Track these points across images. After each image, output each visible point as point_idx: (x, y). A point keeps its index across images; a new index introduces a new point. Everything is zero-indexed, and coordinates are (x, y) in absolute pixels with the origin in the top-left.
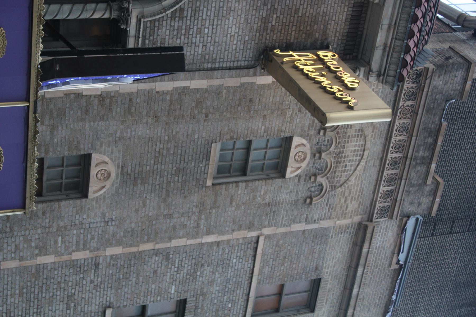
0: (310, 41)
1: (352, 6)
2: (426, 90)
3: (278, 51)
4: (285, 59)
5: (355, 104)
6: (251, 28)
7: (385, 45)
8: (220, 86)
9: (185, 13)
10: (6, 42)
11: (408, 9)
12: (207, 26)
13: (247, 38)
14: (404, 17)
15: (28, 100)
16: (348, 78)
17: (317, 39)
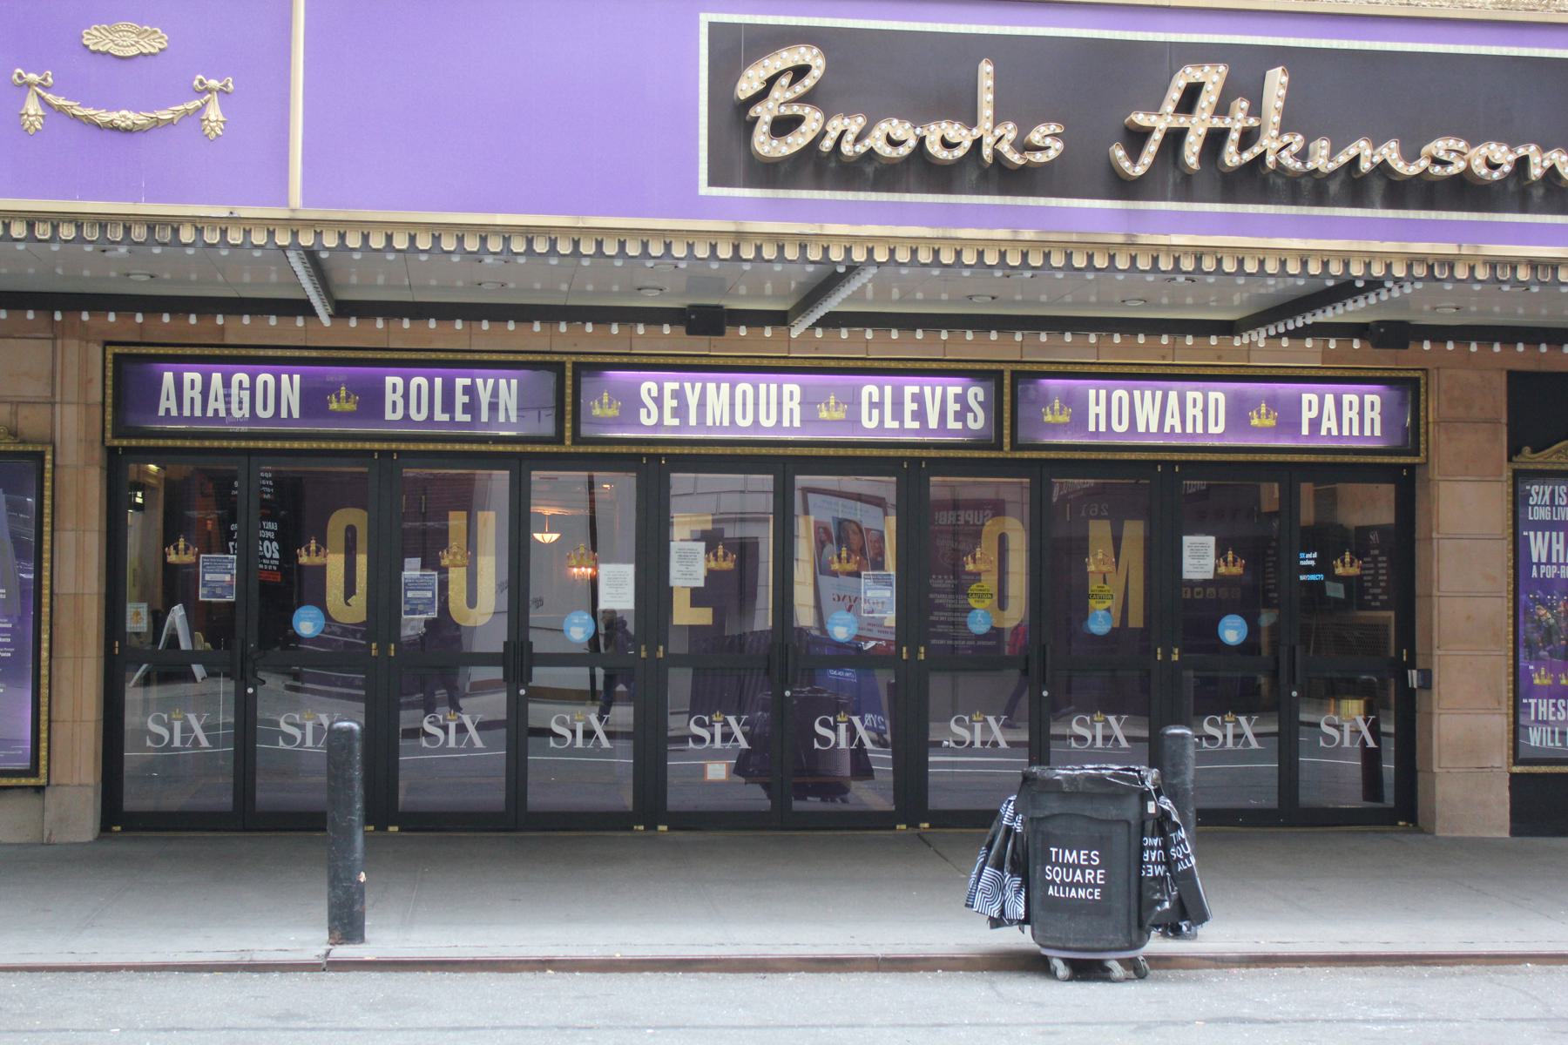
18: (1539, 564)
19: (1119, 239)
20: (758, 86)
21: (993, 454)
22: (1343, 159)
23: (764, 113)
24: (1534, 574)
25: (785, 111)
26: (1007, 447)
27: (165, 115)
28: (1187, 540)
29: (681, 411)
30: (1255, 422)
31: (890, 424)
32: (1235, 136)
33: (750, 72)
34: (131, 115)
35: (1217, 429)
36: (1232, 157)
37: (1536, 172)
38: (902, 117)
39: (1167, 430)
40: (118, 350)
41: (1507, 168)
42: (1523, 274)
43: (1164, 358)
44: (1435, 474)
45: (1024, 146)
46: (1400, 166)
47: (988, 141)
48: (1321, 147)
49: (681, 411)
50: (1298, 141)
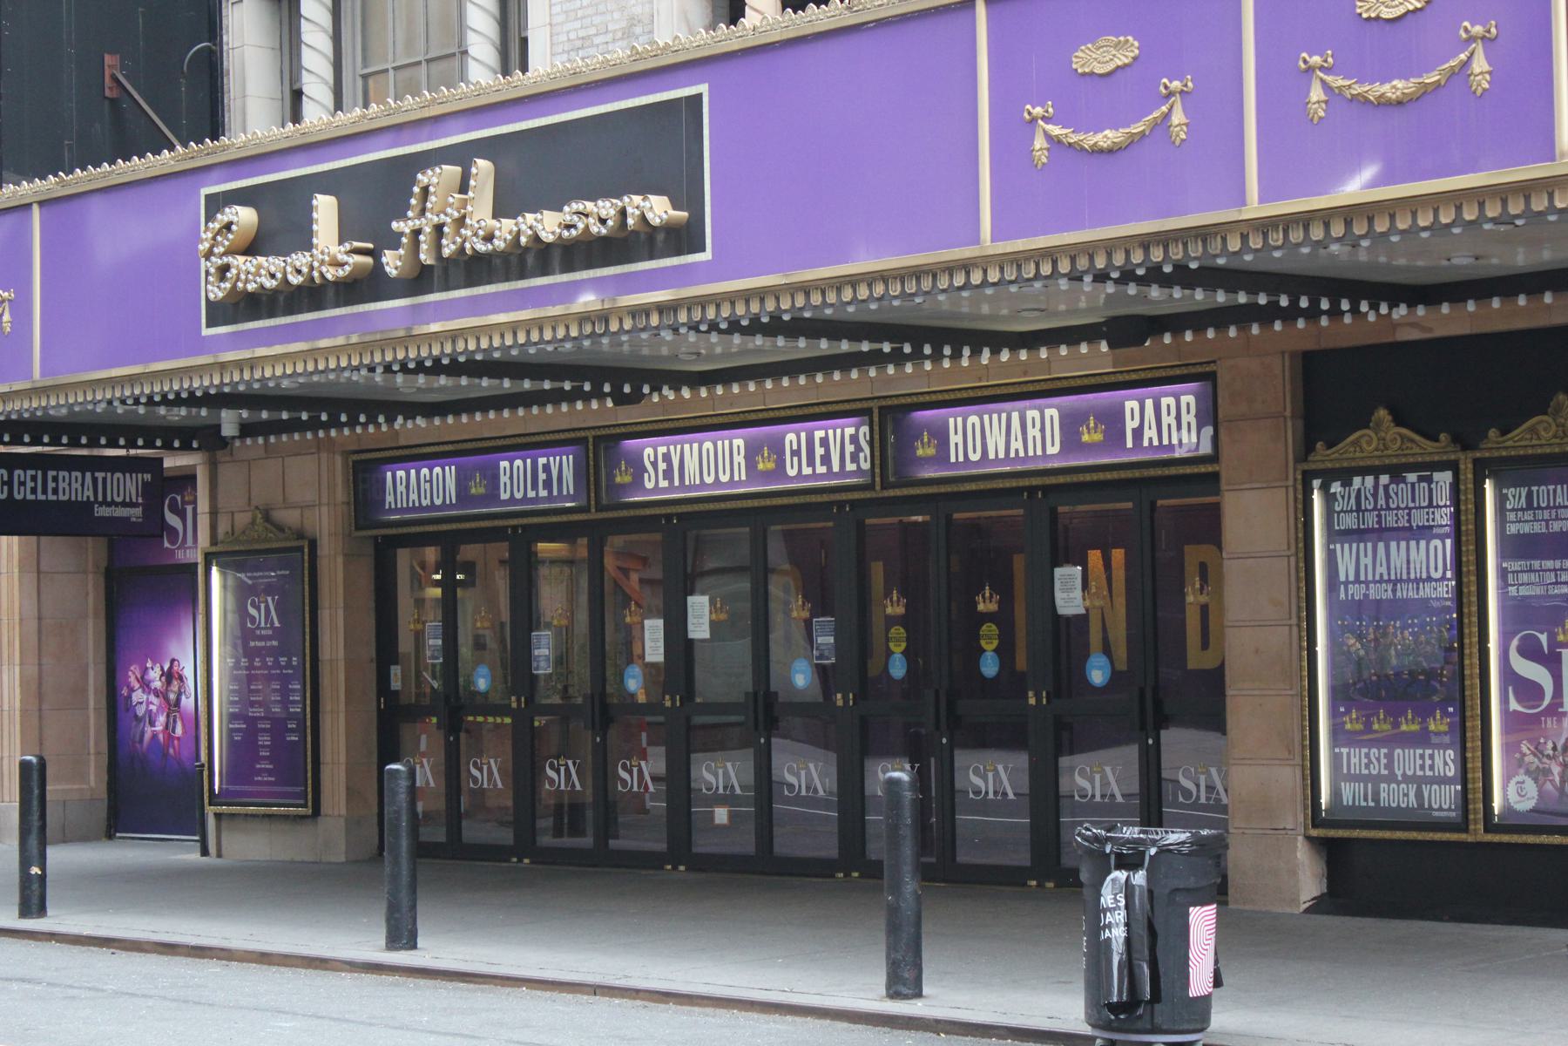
18: (1347, 583)
19: (401, 333)
21: (868, 495)
24: (1342, 596)
26: (878, 487)
28: (1058, 572)
29: (668, 474)
30: (1086, 438)
31: (807, 471)
35: (1053, 450)
39: (1012, 455)
40: (355, 457)
42: (655, 320)
43: (980, 380)
44: (1224, 486)
49: (668, 474)
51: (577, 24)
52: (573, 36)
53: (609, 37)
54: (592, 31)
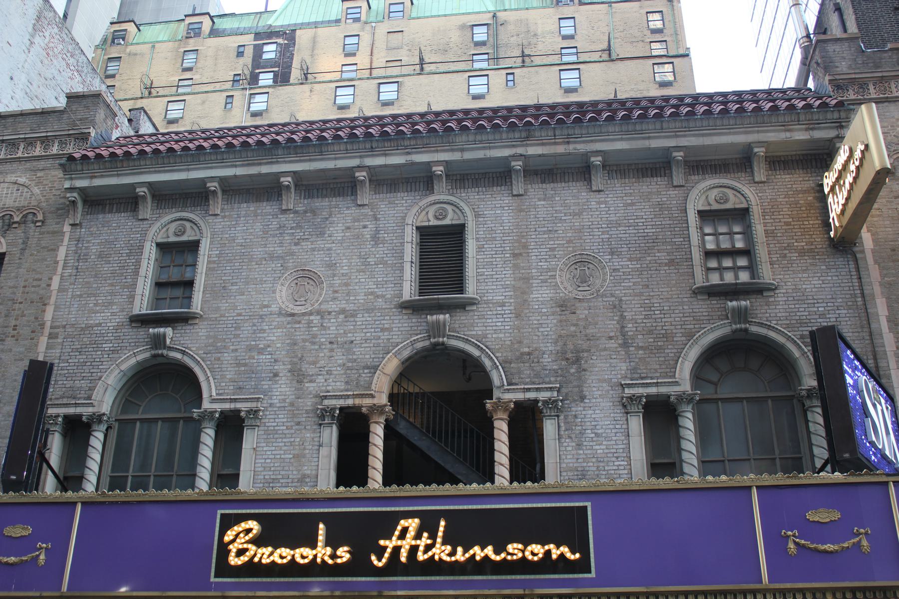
0: (817, 205)
1: (774, 173)
2: (853, 76)
3: (832, 234)
4: (837, 224)
5: (862, 143)
6: (812, 265)
7: (807, 130)
8: (881, 284)
9: (804, 333)
10: (821, 510)
11: (765, 118)
12: (816, 309)
13: (824, 267)
14: (774, 119)
15: (887, 483)
16: (841, 158)
17: (815, 198)
19: (375, 593)
20: (231, 538)
22: (467, 555)
23: (233, 548)
25: (241, 547)
27: (24, 558)
32: (421, 548)
33: (229, 532)
34: (13, 558)
36: (421, 557)
37: (554, 557)
38: (286, 547)
41: (541, 556)
45: (333, 556)
46: (493, 557)
47: (319, 555)
48: (460, 550)
50: (449, 548)
51: (271, 473)
52: (267, 477)
53: (290, 481)
54: (280, 477)
